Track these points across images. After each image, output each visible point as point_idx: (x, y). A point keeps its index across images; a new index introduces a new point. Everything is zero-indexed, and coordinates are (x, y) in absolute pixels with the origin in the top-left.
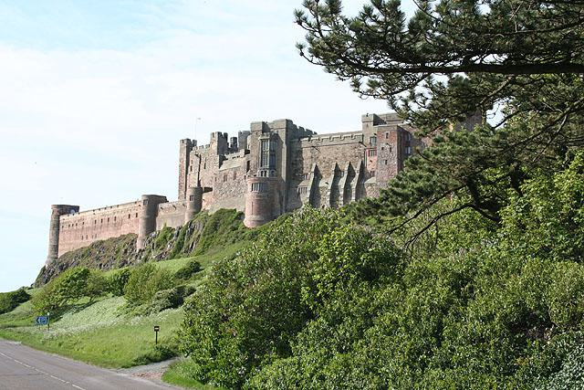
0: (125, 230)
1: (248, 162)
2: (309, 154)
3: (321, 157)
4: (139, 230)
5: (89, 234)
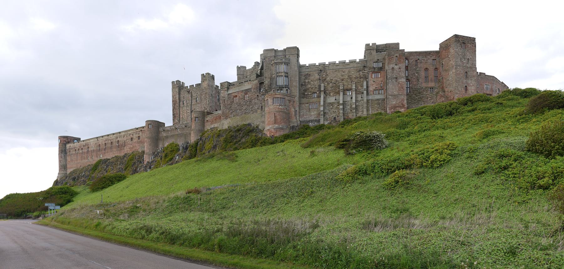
0: (127, 150)
1: (261, 83)
2: (317, 77)
3: (328, 79)
4: (147, 147)
5: (94, 154)
